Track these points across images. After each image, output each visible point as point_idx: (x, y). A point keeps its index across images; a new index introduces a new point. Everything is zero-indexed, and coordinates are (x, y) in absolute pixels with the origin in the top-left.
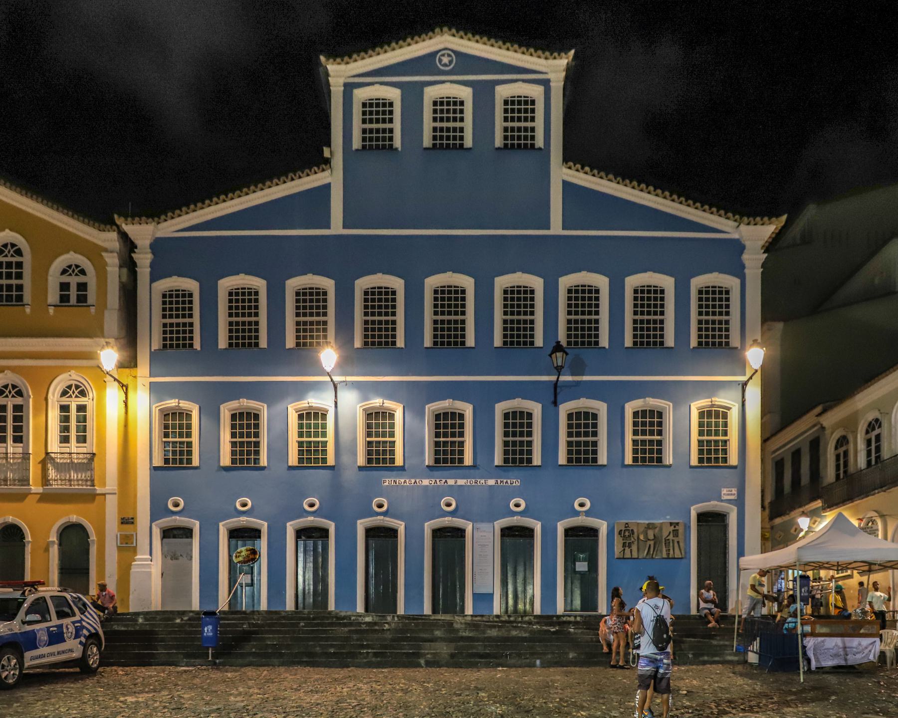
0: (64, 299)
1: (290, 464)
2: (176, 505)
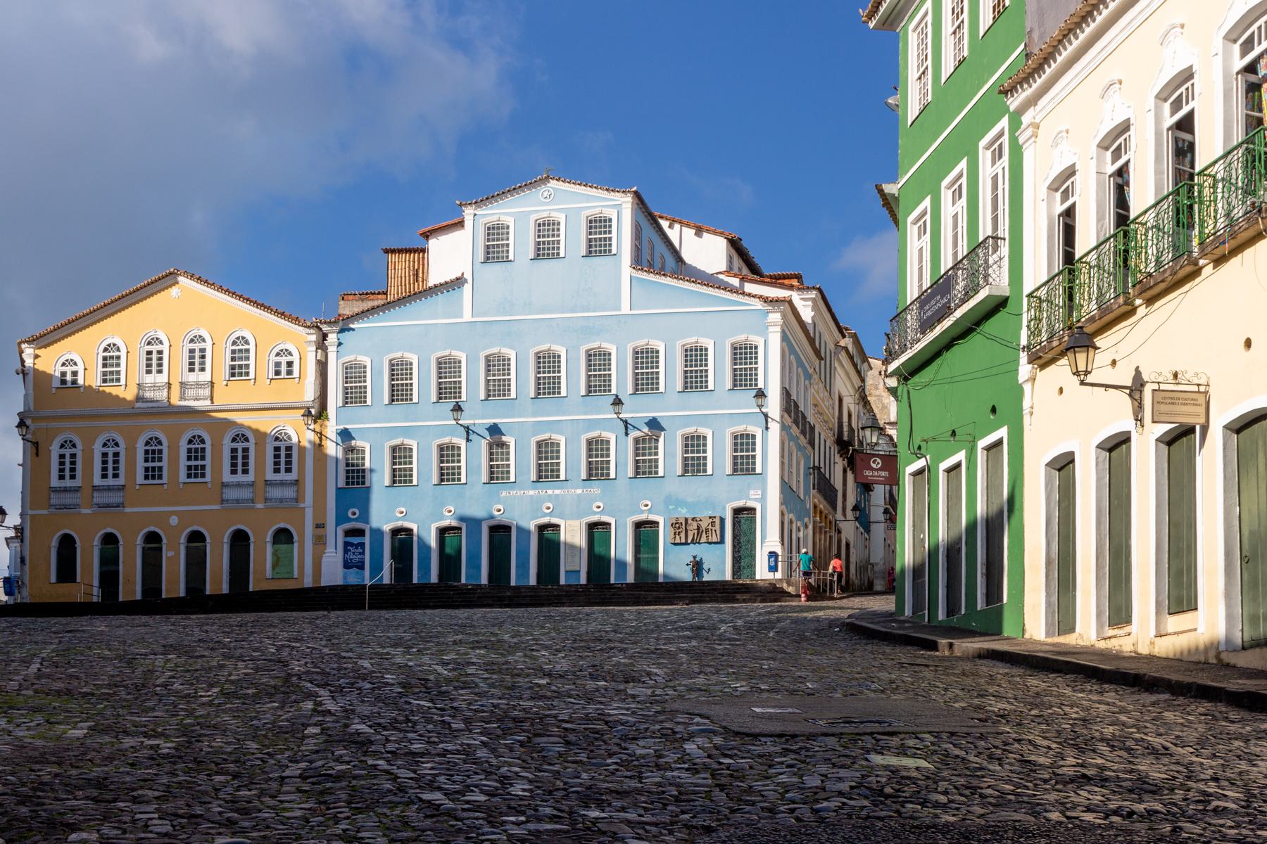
0: (278, 373)
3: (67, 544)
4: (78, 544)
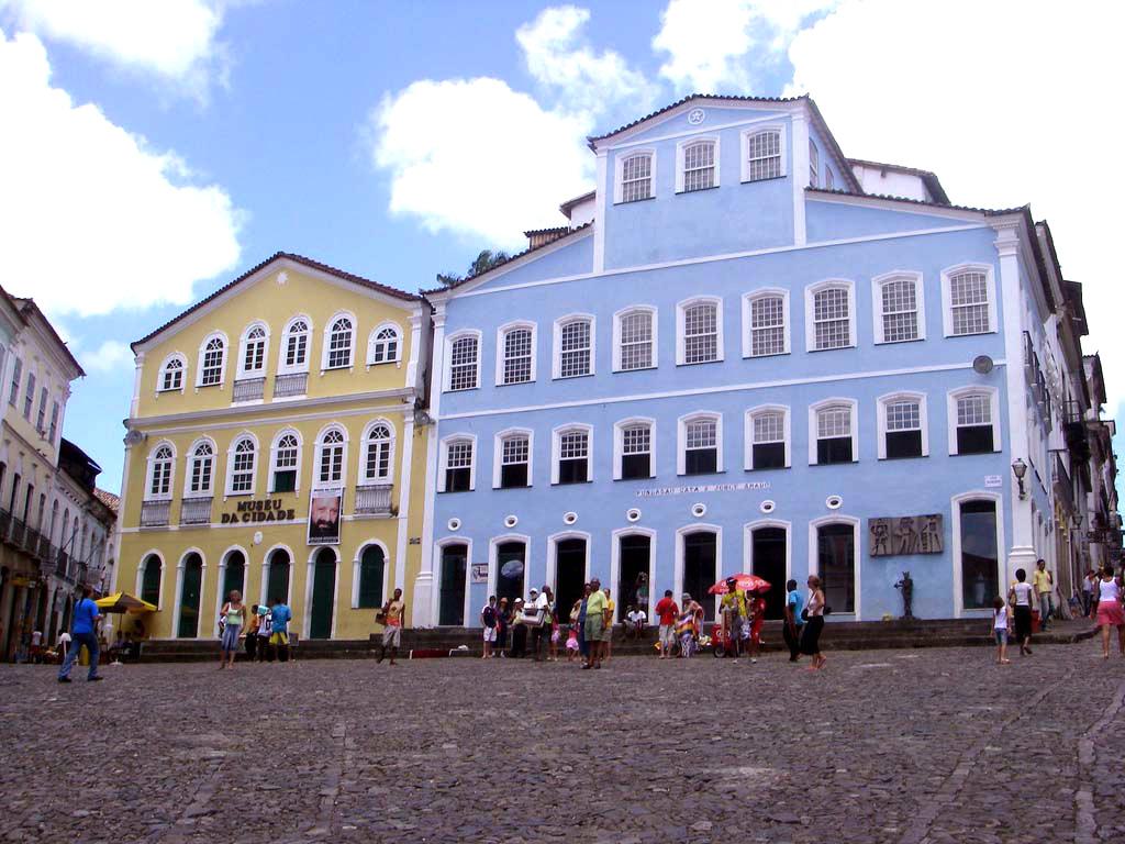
0: (379, 357)
1: (553, 483)
2: (455, 525)
3: (153, 564)
4: (163, 566)
